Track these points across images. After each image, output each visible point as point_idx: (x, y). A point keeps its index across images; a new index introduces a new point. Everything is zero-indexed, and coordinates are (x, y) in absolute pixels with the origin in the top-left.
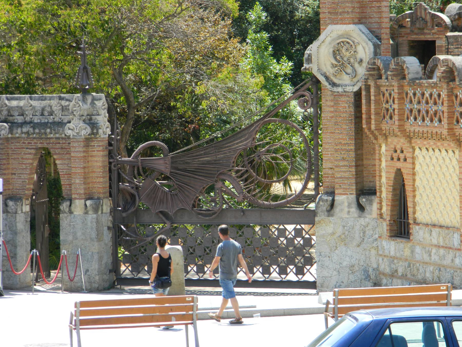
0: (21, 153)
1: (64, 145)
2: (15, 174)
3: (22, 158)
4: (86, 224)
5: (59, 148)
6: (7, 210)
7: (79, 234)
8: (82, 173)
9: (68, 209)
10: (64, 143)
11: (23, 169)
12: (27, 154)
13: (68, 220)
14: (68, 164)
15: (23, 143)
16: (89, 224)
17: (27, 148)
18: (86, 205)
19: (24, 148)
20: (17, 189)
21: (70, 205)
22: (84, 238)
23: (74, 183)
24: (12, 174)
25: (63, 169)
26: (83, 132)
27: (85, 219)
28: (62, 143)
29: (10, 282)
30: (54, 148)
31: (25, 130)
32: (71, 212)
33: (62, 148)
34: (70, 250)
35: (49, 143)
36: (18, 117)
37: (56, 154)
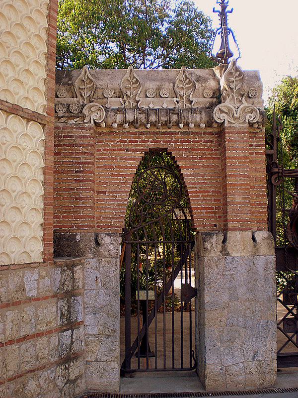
0: (116, 158)
1: (197, 144)
2: (104, 193)
3: (119, 167)
4: (256, 273)
5: (186, 150)
6: (99, 251)
7: (241, 291)
8: (248, 185)
9: (220, 247)
10: (198, 142)
11: (118, 184)
12: (127, 159)
13: (221, 266)
14: (204, 175)
15: (121, 141)
16: (261, 271)
17: (128, 150)
18: (254, 239)
19: (124, 150)
20: (107, 218)
21: (224, 241)
22: (252, 297)
23: (232, 202)
24: (99, 193)
25: (195, 184)
26: (249, 117)
27: (254, 264)
28: (193, 142)
29: (102, 381)
30: (180, 150)
31: (130, 117)
32: (225, 253)
33: (193, 150)
34: (224, 319)
35: (170, 142)
36: (113, 99)
37: (182, 159)
